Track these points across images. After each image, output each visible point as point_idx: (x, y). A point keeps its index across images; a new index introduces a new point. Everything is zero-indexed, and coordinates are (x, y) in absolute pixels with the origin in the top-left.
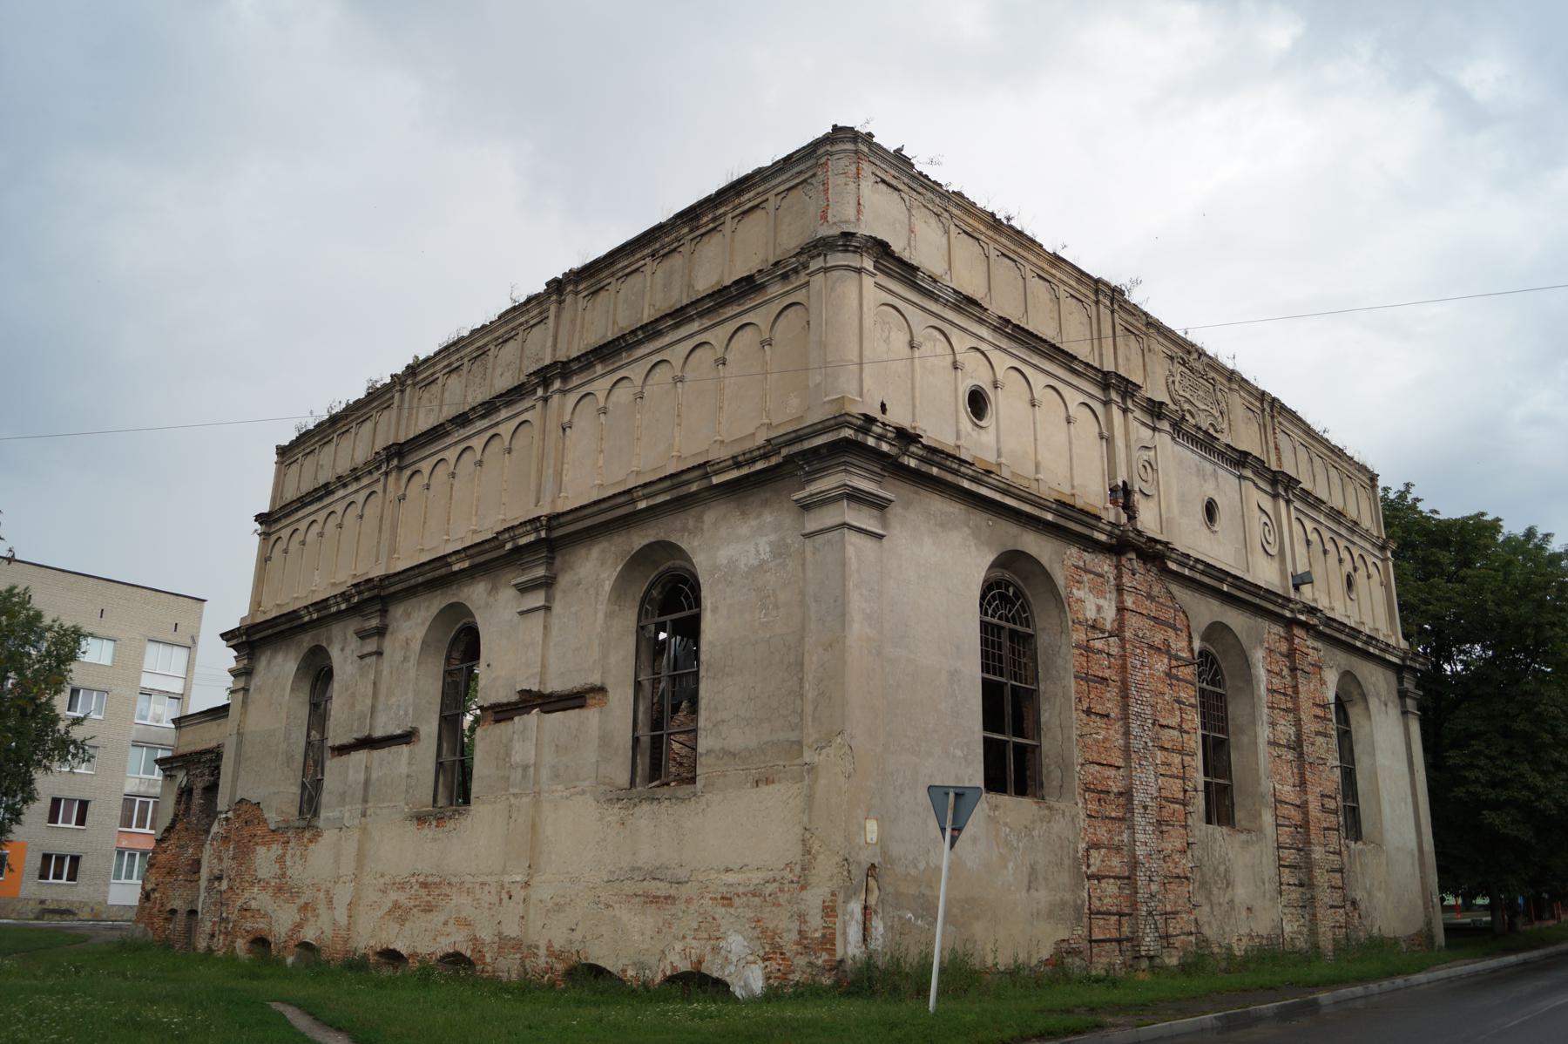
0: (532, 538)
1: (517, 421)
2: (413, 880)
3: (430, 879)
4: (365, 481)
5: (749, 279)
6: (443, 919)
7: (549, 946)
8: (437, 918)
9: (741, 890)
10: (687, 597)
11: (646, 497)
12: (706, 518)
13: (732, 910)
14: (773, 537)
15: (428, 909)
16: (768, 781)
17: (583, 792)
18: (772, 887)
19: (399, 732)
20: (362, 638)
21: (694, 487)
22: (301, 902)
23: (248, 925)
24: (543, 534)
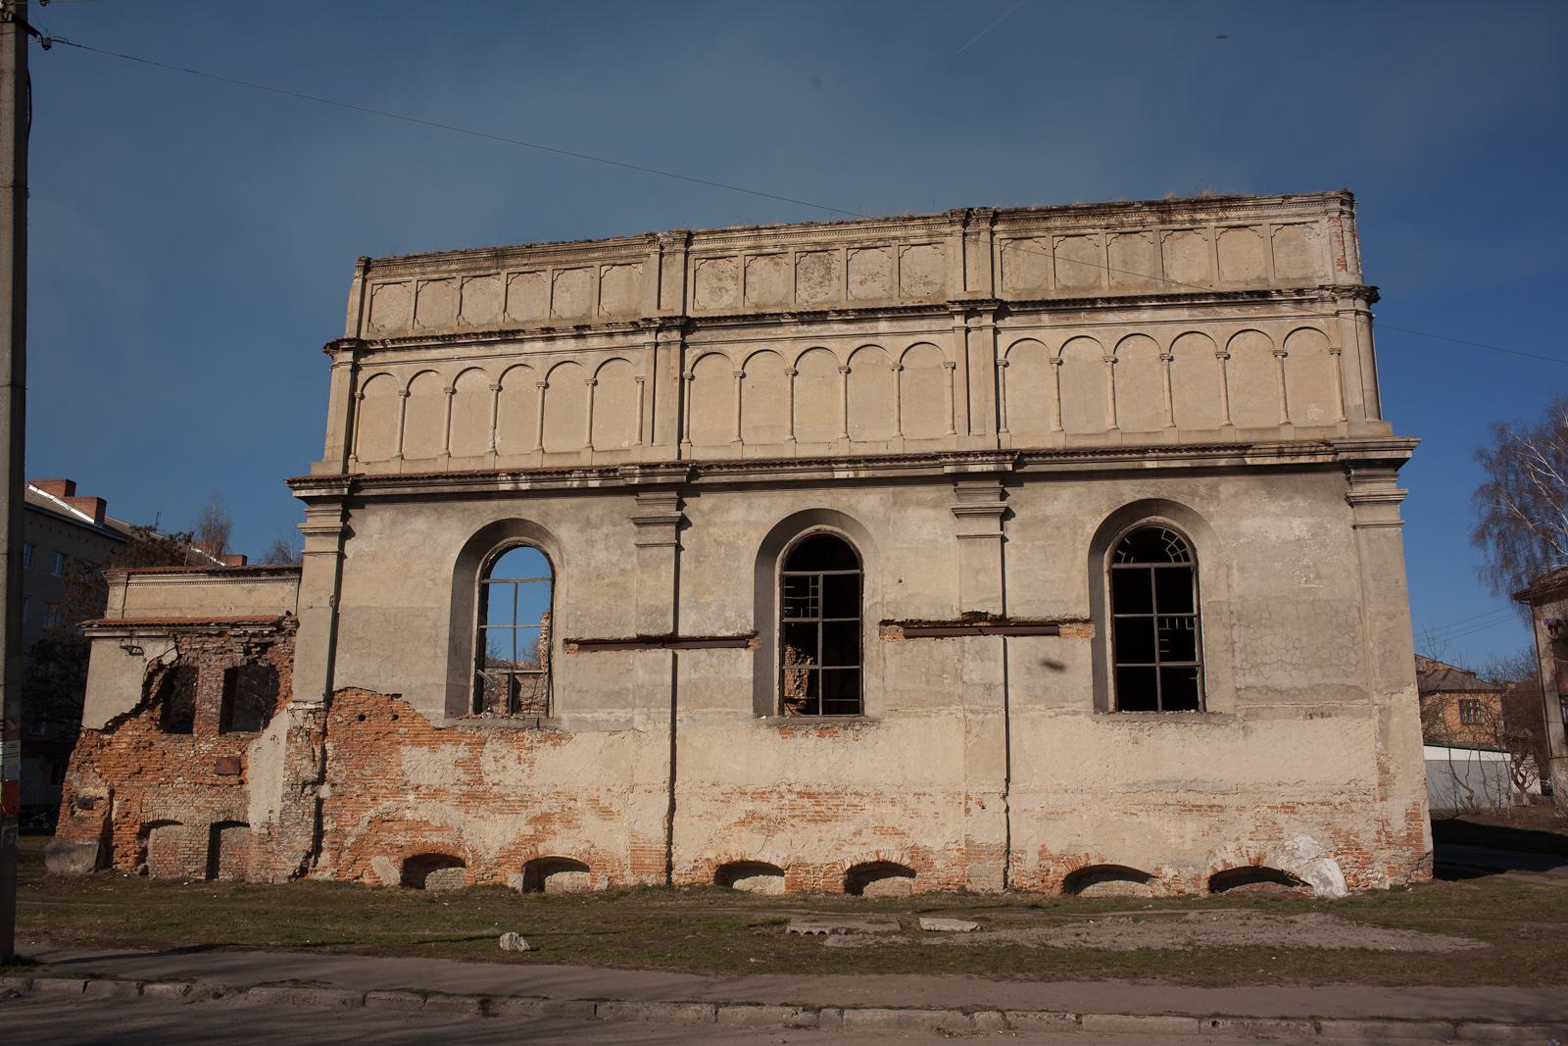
0: (991, 468)
1: (912, 340)
2: (783, 788)
3: (814, 789)
4: (594, 342)
5: (1265, 294)
6: (853, 828)
7: (1043, 853)
8: (843, 829)
9: (1304, 800)
10: (1173, 550)
11: (1158, 459)
12: (1221, 488)
13: (1297, 817)
14: (1309, 520)
15: (820, 819)
16: (1322, 715)
17: (1075, 713)
18: (1343, 798)
19: (729, 634)
20: (637, 524)
21: (1222, 462)
22: (536, 810)
23: (401, 840)
24: (1010, 467)
